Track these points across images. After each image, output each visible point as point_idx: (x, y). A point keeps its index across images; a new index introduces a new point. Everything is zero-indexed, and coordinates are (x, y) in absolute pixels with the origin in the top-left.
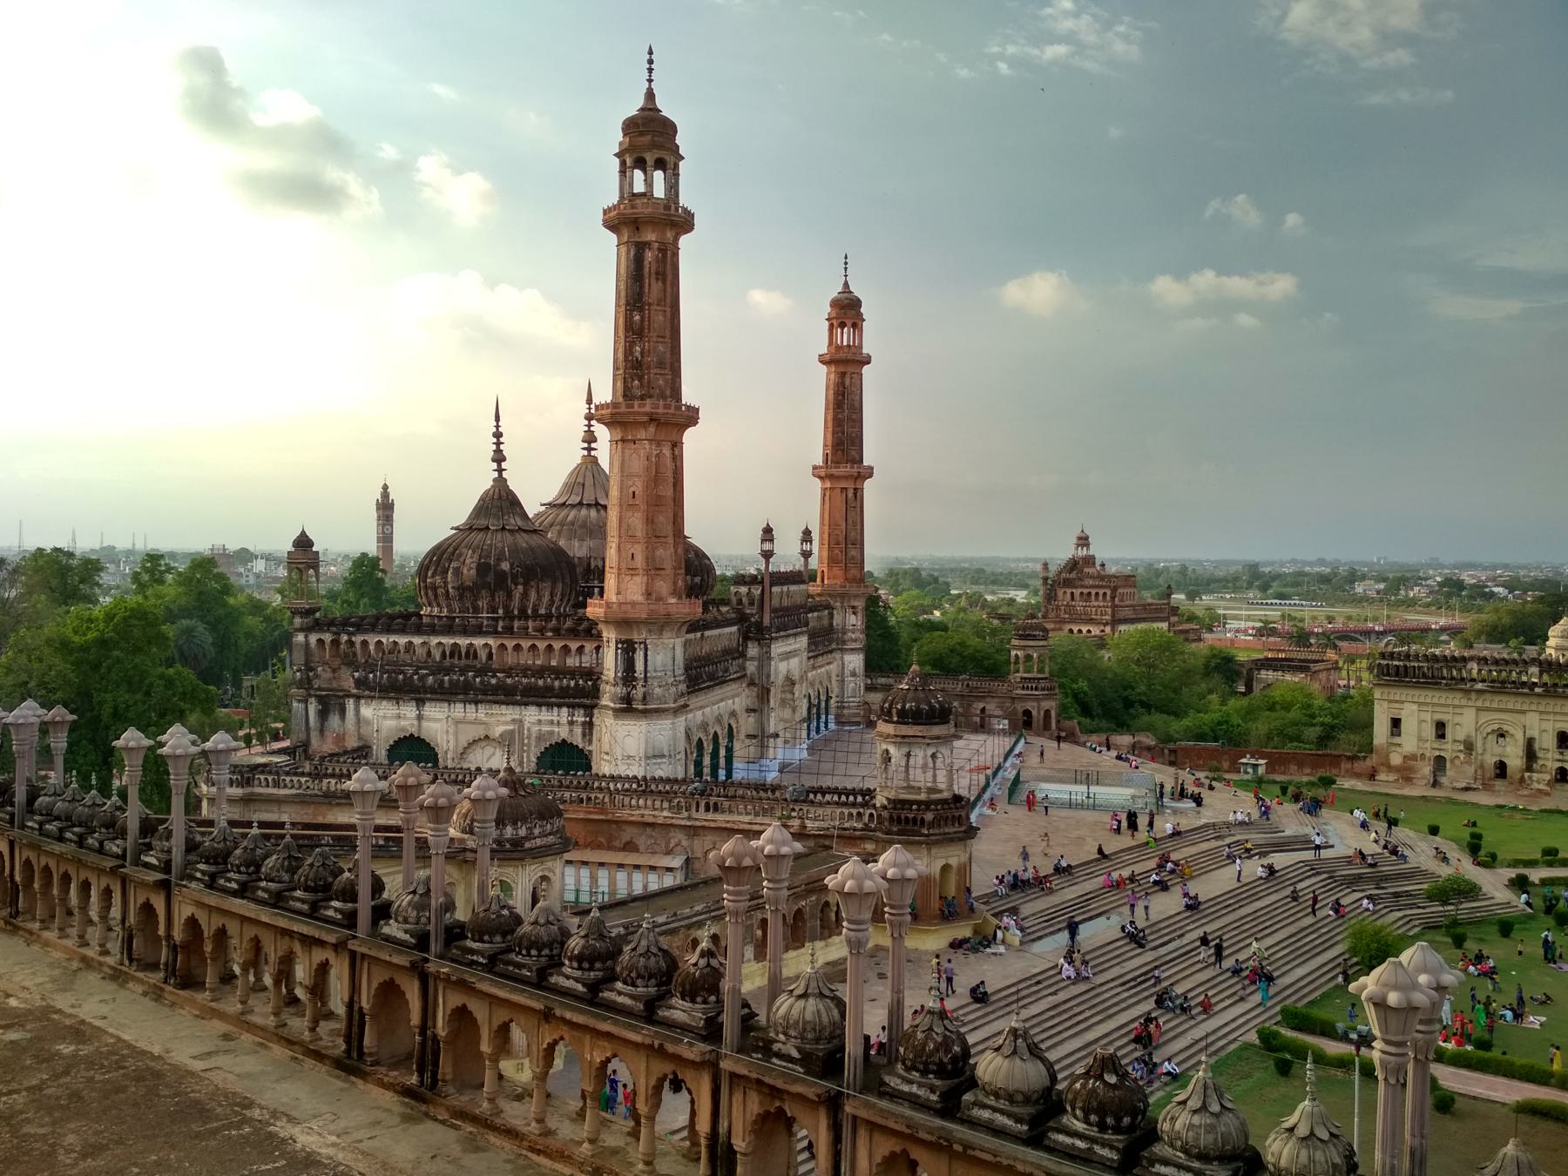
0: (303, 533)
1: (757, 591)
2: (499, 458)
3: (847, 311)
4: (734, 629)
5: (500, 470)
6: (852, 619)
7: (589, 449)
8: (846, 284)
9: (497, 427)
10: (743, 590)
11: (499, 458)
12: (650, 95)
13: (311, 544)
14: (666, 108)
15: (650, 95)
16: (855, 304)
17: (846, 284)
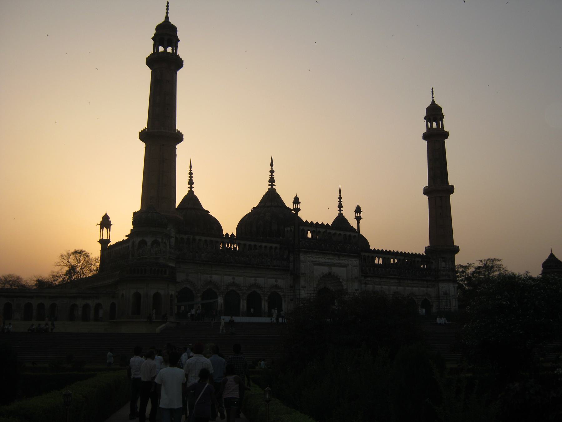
0: (106, 214)
1: (293, 229)
2: (191, 183)
3: (434, 113)
4: (274, 245)
5: (191, 188)
6: (443, 264)
7: (272, 185)
8: (433, 101)
9: (191, 170)
10: (289, 229)
11: (191, 183)
12: (167, 18)
13: (109, 218)
14: (172, 21)
15: (167, 18)
16: (440, 109)
17: (433, 101)
